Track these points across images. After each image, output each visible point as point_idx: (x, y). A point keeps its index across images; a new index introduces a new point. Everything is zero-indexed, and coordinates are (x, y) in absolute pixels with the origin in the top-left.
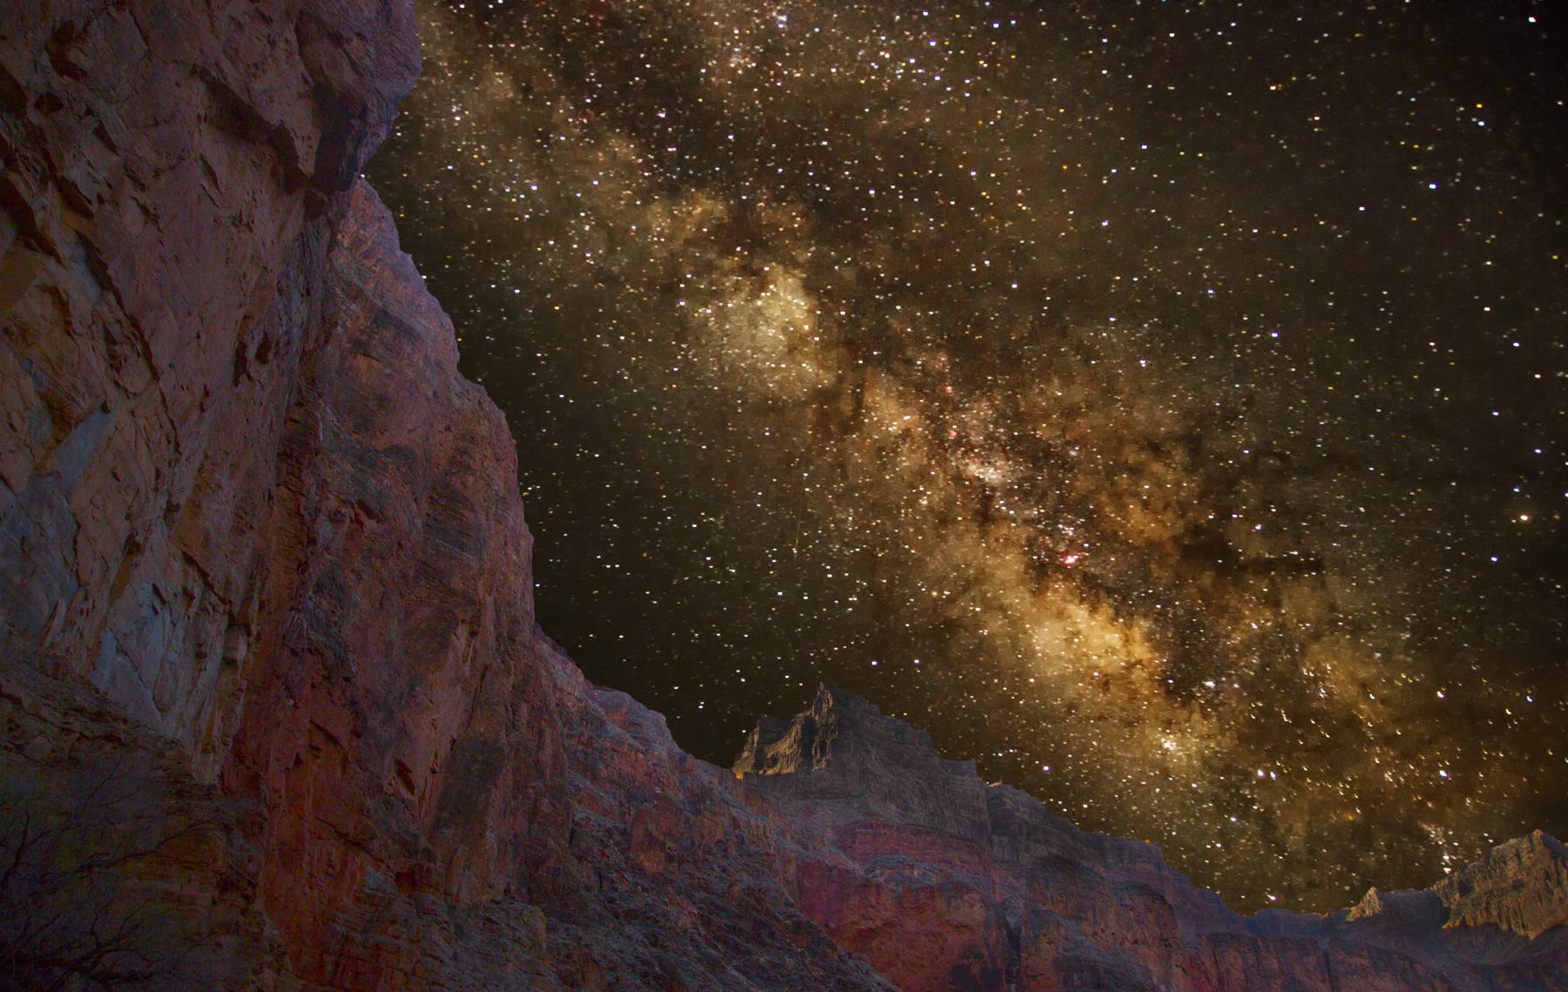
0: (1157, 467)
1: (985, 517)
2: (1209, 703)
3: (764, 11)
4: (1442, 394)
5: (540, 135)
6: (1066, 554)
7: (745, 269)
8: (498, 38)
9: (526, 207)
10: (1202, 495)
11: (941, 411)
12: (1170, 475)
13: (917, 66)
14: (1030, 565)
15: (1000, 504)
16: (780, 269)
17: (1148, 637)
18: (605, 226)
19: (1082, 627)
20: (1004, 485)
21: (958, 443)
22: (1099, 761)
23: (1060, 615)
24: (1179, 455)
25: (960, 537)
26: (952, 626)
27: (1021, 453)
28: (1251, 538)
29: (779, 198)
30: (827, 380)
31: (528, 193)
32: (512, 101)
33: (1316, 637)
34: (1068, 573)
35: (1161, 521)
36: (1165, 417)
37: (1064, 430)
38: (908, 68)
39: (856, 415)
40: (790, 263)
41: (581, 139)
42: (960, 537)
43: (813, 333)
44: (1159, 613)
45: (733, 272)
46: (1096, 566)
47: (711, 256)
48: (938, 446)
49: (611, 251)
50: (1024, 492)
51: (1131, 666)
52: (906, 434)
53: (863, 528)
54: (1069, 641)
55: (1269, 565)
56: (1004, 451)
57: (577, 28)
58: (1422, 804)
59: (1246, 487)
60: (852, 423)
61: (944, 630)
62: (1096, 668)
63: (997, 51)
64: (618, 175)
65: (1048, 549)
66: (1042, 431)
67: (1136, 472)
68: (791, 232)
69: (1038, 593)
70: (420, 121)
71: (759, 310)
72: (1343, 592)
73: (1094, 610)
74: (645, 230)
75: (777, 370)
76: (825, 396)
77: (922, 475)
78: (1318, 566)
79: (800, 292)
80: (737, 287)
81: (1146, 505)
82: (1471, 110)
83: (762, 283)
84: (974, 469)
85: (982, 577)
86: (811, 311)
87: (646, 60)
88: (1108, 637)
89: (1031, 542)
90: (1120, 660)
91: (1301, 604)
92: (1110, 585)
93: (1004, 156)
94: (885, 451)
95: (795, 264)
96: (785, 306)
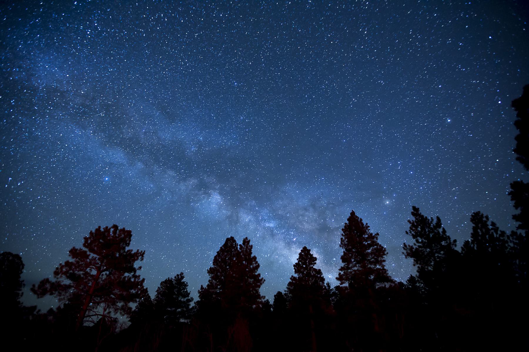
0: (307, 213)
1: (273, 235)
3: (197, 138)
7: (205, 193)
8: (137, 155)
12: (311, 214)
14: (286, 243)
15: (275, 231)
21: (262, 220)
24: (311, 209)
26: (272, 263)
29: (209, 176)
31: (151, 187)
34: (295, 243)
36: (304, 202)
39: (238, 219)
40: (214, 189)
41: (161, 173)
43: (223, 203)
45: (202, 194)
48: (258, 222)
50: (280, 227)
52: (250, 220)
59: (328, 212)
60: (237, 222)
66: (280, 212)
69: (290, 249)
70: (122, 177)
74: (180, 190)
76: (229, 217)
77: (256, 229)
81: (307, 222)
83: (209, 195)
84: (267, 225)
85: (276, 249)
89: (284, 238)
95: (216, 189)
96: (216, 198)
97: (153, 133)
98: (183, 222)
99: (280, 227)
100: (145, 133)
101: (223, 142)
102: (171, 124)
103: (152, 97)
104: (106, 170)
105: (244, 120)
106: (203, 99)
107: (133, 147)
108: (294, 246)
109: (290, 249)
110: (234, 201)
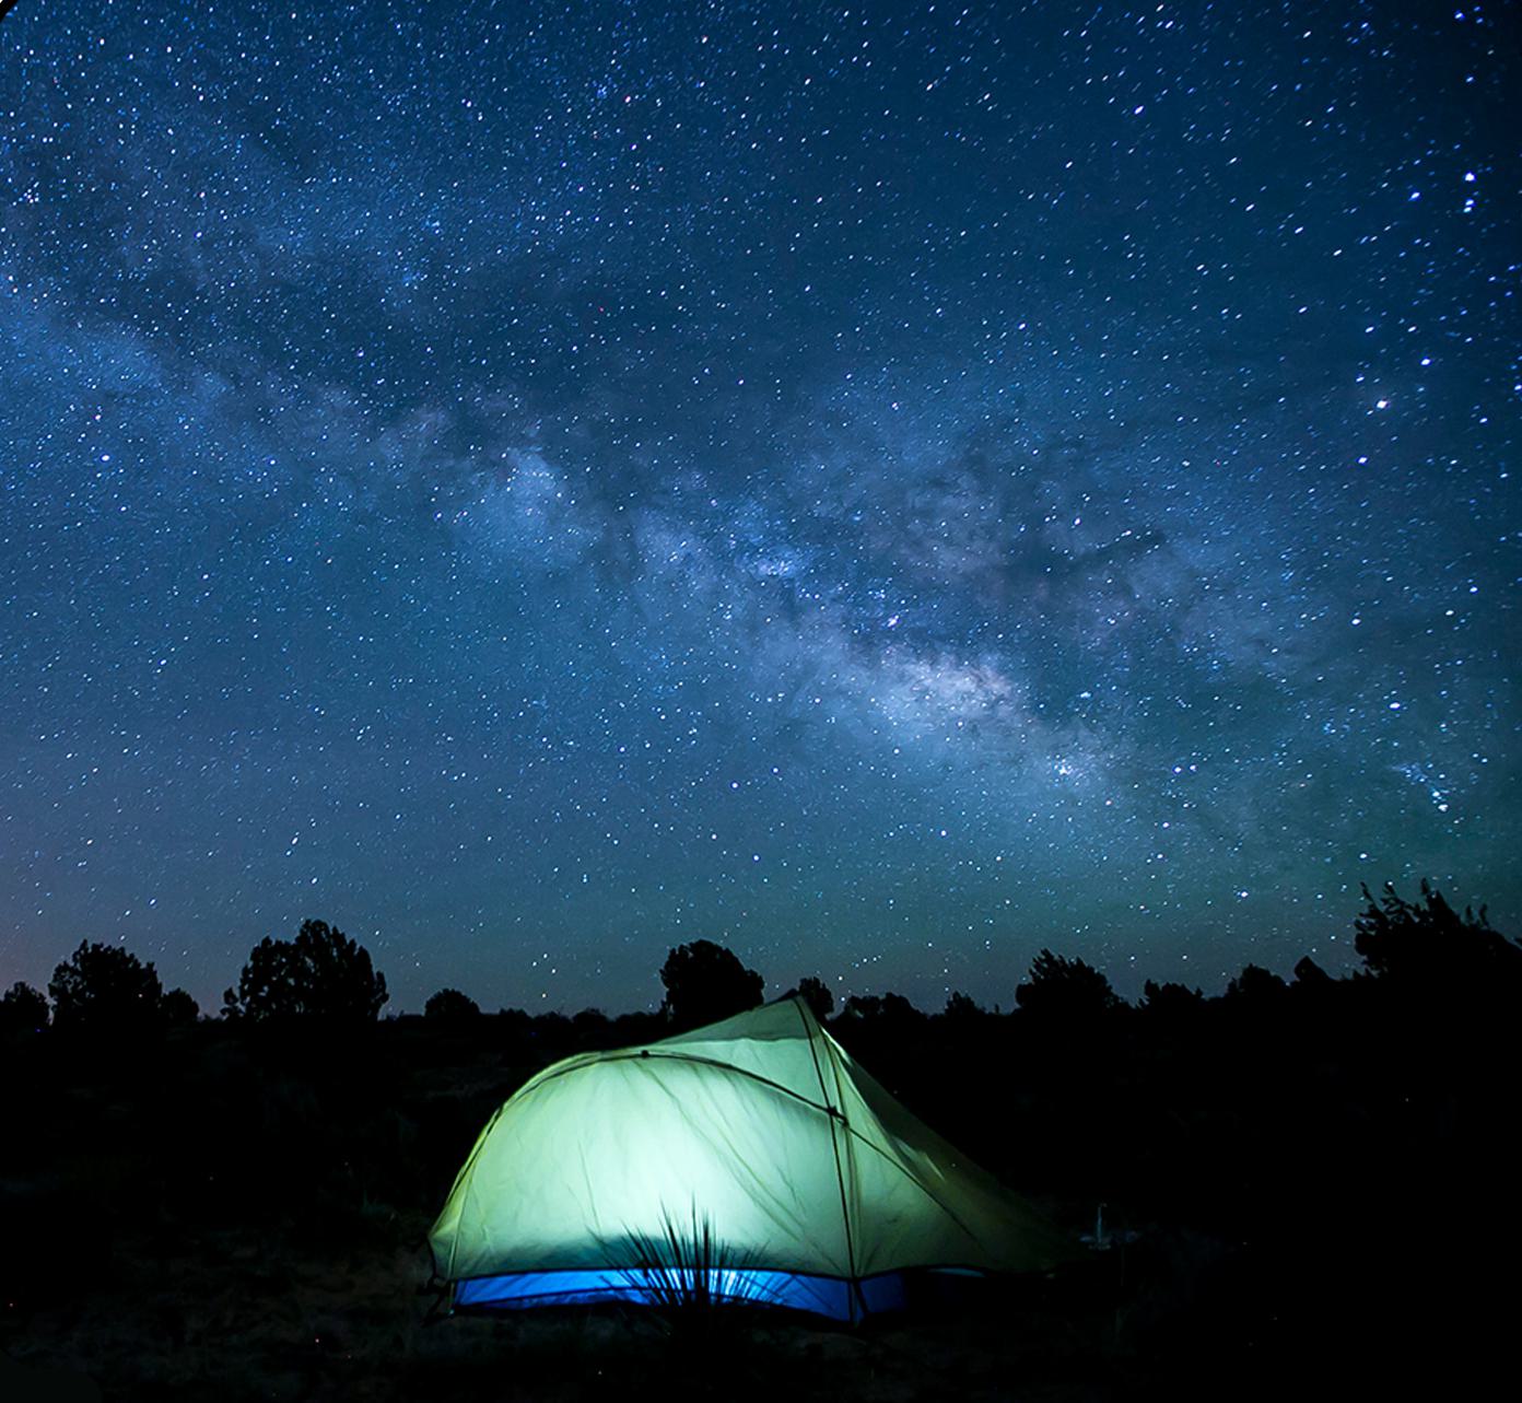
1: (791, 609)
2: (1091, 715)
3: (418, 225)
4: (1231, 314)
5: (262, 414)
7: (487, 463)
9: (271, 482)
10: (1006, 509)
11: (713, 526)
12: (965, 503)
13: (573, 216)
14: (854, 640)
15: (804, 594)
17: (1001, 670)
18: (346, 473)
19: (928, 682)
20: (800, 573)
21: (740, 550)
22: (995, 809)
23: (902, 678)
25: (774, 638)
27: (806, 537)
28: (1074, 535)
29: (490, 388)
30: (596, 536)
32: (228, 393)
33: (1186, 609)
34: (894, 636)
35: (970, 552)
36: (935, 450)
37: (839, 499)
38: (567, 220)
40: (523, 442)
42: (774, 638)
43: (567, 497)
44: (1003, 642)
46: (919, 619)
47: (452, 463)
48: (723, 559)
49: (359, 492)
50: (820, 574)
51: (993, 706)
52: (688, 558)
53: (679, 661)
55: (1103, 555)
56: (788, 542)
57: (259, 308)
58: (1385, 745)
59: (1049, 487)
60: (635, 566)
61: (789, 733)
62: (959, 718)
63: (644, 172)
64: (340, 423)
65: (865, 619)
66: (820, 508)
67: (927, 514)
69: (873, 664)
72: (1197, 554)
73: (934, 663)
74: (382, 462)
76: (599, 553)
77: (717, 593)
78: (1158, 538)
79: (543, 465)
80: (484, 482)
81: (949, 542)
82: (1153, 17)
83: (505, 469)
84: (765, 569)
85: (810, 668)
86: (558, 478)
87: (329, 311)
88: (958, 684)
90: (978, 704)
91: (1155, 579)
92: (943, 632)
93: (687, 265)
95: (530, 442)
96: (535, 477)
97: (236, 238)
99: (820, 574)
100: (206, 244)
101: (532, 224)
102: (302, 185)
103: (203, 76)
104: (96, 425)
105: (614, 100)
106: (416, 38)
107: (168, 310)
108: (892, 650)
109: (873, 664)
110: (615, 489)
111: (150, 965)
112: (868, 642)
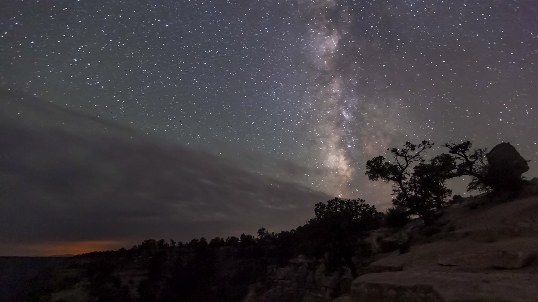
6: (349, 144)
7: (329, 27)
16: (336, 32)
17: (352, 173)
21: (345, 104)
29: (350, 12)
40: (340, 33)
43: (333, 55)
48: (340, 102)
50: (350, 125)
51: (344, 176)
52: (336, 94)
53: (311, 109)
54: (336, 162)
61: (313, 142)
66: (365, 114)
67: (377, 137)
68: (346, 23)
69: (338, 148)
71: (325, 40)
73: (345, 160)
75: (319, 58)
76: (325, 73)
77: (332, 106)
79: (337, 42)
80: (324, 30)
81: (373, 146)
83: (330, 33)
84: (344, 113)
85: (328, 137)
86: (336, 49)
90: (343, 173)
94: (329, 95)
96: (332, 43)
98: (286, 33)
99: (350, 125)
109: (338, 148)
110: (341, 64)
111: (374, 206)
112: (341, 144)
